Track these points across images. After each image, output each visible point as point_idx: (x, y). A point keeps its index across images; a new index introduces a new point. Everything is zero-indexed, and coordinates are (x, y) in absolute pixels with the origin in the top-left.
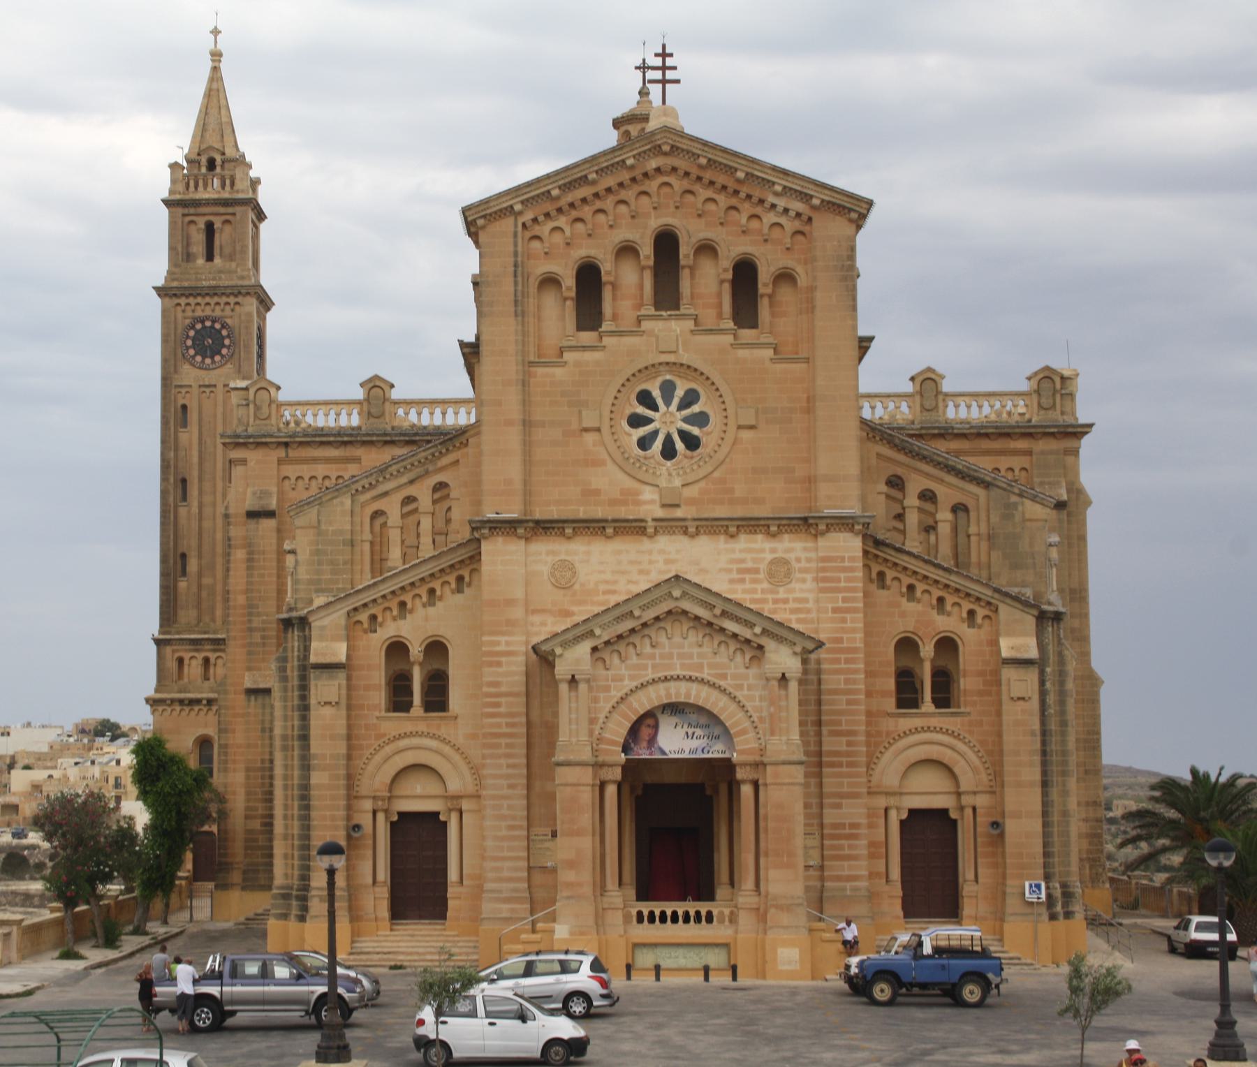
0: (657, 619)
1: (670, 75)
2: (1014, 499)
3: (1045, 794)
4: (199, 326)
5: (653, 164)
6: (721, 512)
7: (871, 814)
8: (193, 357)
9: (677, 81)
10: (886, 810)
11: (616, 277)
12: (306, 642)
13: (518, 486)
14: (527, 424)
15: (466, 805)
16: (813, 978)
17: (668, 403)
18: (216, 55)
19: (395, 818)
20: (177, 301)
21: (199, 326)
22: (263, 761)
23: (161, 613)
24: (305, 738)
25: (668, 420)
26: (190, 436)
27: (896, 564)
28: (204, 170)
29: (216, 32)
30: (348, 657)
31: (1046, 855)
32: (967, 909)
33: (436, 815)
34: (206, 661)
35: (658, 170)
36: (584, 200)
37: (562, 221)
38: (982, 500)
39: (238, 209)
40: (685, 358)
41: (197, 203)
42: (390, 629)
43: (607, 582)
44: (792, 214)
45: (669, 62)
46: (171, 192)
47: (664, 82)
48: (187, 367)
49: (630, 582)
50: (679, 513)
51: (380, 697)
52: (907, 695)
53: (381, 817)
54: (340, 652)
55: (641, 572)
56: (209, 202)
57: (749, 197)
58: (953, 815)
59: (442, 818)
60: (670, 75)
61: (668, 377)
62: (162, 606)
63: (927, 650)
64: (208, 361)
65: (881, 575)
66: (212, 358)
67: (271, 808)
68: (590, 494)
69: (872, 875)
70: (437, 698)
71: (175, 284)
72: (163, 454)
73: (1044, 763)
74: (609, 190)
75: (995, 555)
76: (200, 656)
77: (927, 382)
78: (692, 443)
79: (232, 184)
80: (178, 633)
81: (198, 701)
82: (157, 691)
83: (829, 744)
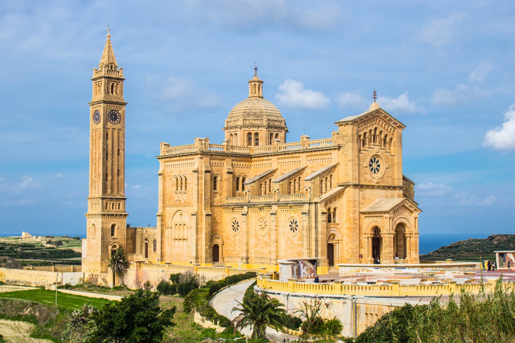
2: (410, 183)
5: (376, 115)
6: (383, 184)
13: (357, 177)
15: (340, 242)
20: (107, 105)
21: (112, 112)
23: (103, 190)
25: (375, 165)
33: (332, 244)
34: (113, 203)
39: (121, 82)
47: (375, 98)
48: (109, 123)
49: (372, 198)
55: (373, 196)
62: (103, 189)
64: (114, 122)
66: (115, 121)
68: (366, 179)
71: (106, 100)
72: (103, 146)
76: (112, 202)
80: (107, 196)
81: (113, 215)
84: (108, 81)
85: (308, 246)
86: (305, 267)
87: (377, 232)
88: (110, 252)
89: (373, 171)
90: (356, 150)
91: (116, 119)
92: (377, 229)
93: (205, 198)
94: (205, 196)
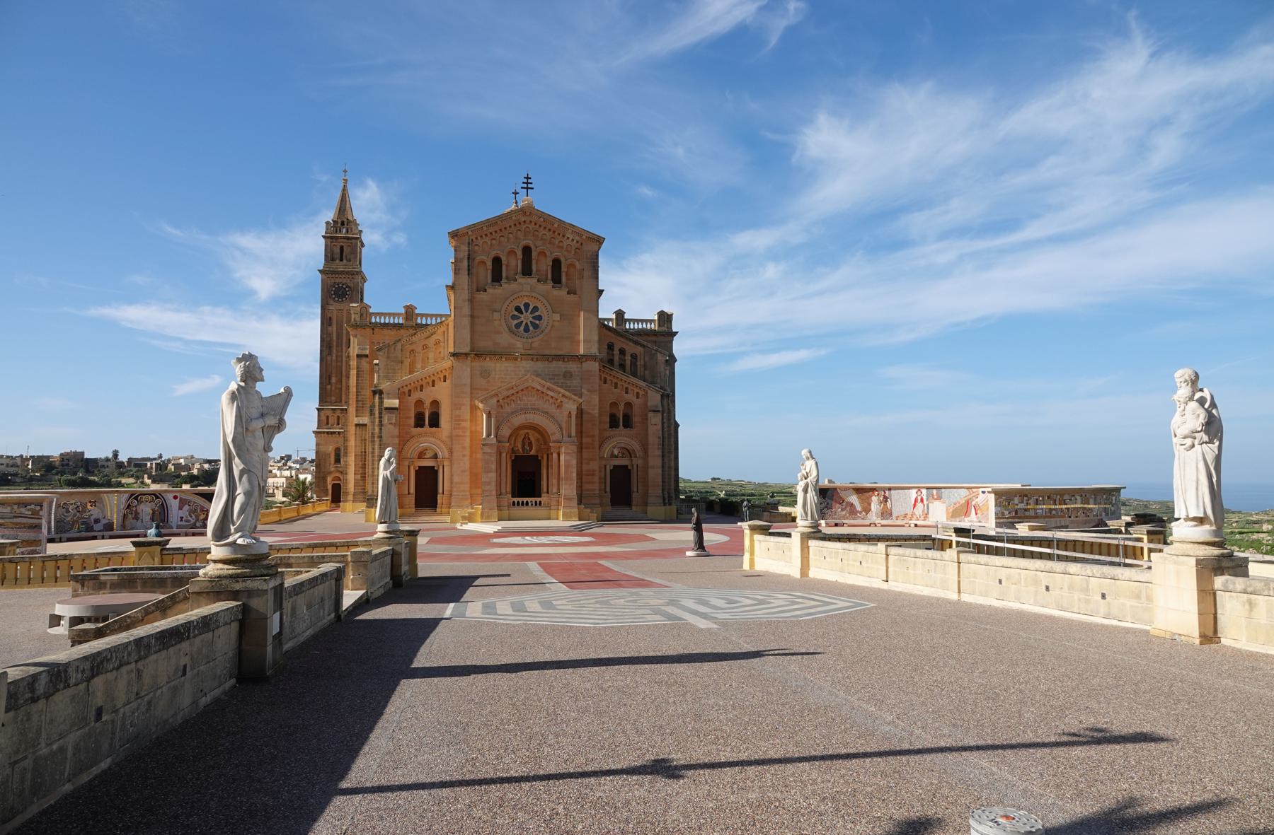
0: (522, 390)
1: (530, 186)
3: (663, 460)
4: (337, 286)
6: (547, 352)
7: (600, 467)
8: (334, 298)
9: (532, 188)
10: (605, 466)
11: (508, 262)
12: (381, 400)
14: (472, 317)
16: (580, 520)
17: (527, 312)
18: (346, 181)
19: (417, 469)
22: (362, 452)
24: (380, 437)
25: (527, 318)
26: (334, 329)
27: (611, 375)
28: (339, 225)
29: (345, 171)
30: (399, 405)
31: (663, 482)
32: (634, 503)
33: (434, 467)
34: (338, 417)
35: (524, 222)
36: (496, 232)
37: (486, 239)
38: (642, 352)
39: (353, 241)
40: (534, 294)
41: (337, 238)
42: (417, 395)
43: (502, 378)
44: (575, 241)
45: (529, 181)
46: (326, 233)
47: (527, 188)
48: (331, 302)
50: (530, 352)
51: (412, 421)
52: (614, 423)
53: (412, 468)
54: (395, 403)
56: (341, 238)
57: (559, 234)
58: (629, 468)
59: (436, 468)
60: (530, 186)
61: (527, 301)
63: (622, 407)
65: (605, 378)
67: (365, 470)
69: (600, 490)
70: (435, 422)
73: (663, 449)
74: (505, 228)
75: (647, 372)
77: (620, 314)
78: (536, 327)
79: (352, 231)
82: (317, 429)
83: (585, 440)
84: (331, 242)
85: (369, 471)
86: (186, 507)
87: (527, 444)
88: (330, 487)
89: (522, 328)
90: (466, 287)
91: (344, 295)
92: (529, 439)
93: (357, 398)
94: (357, 395)
